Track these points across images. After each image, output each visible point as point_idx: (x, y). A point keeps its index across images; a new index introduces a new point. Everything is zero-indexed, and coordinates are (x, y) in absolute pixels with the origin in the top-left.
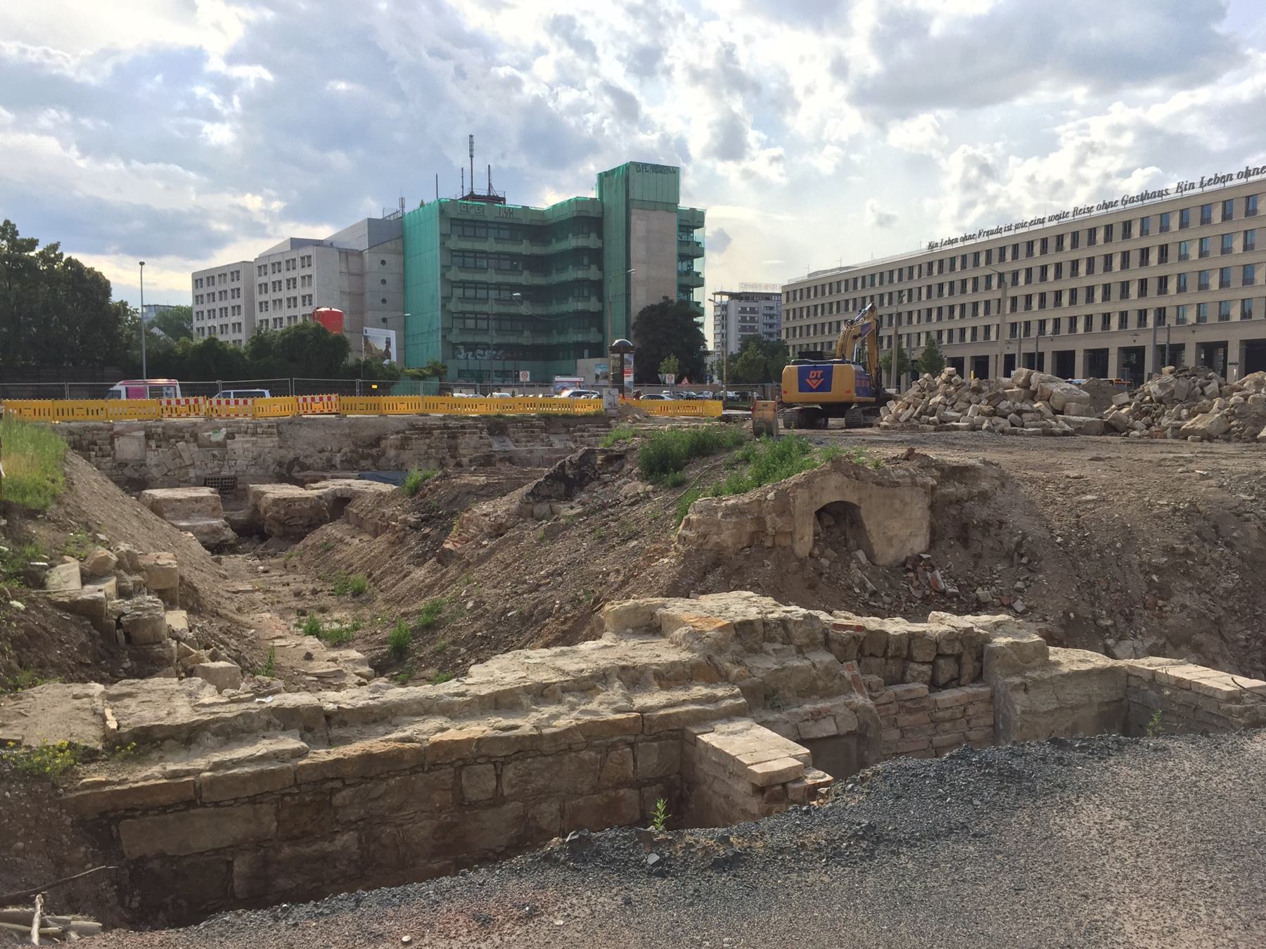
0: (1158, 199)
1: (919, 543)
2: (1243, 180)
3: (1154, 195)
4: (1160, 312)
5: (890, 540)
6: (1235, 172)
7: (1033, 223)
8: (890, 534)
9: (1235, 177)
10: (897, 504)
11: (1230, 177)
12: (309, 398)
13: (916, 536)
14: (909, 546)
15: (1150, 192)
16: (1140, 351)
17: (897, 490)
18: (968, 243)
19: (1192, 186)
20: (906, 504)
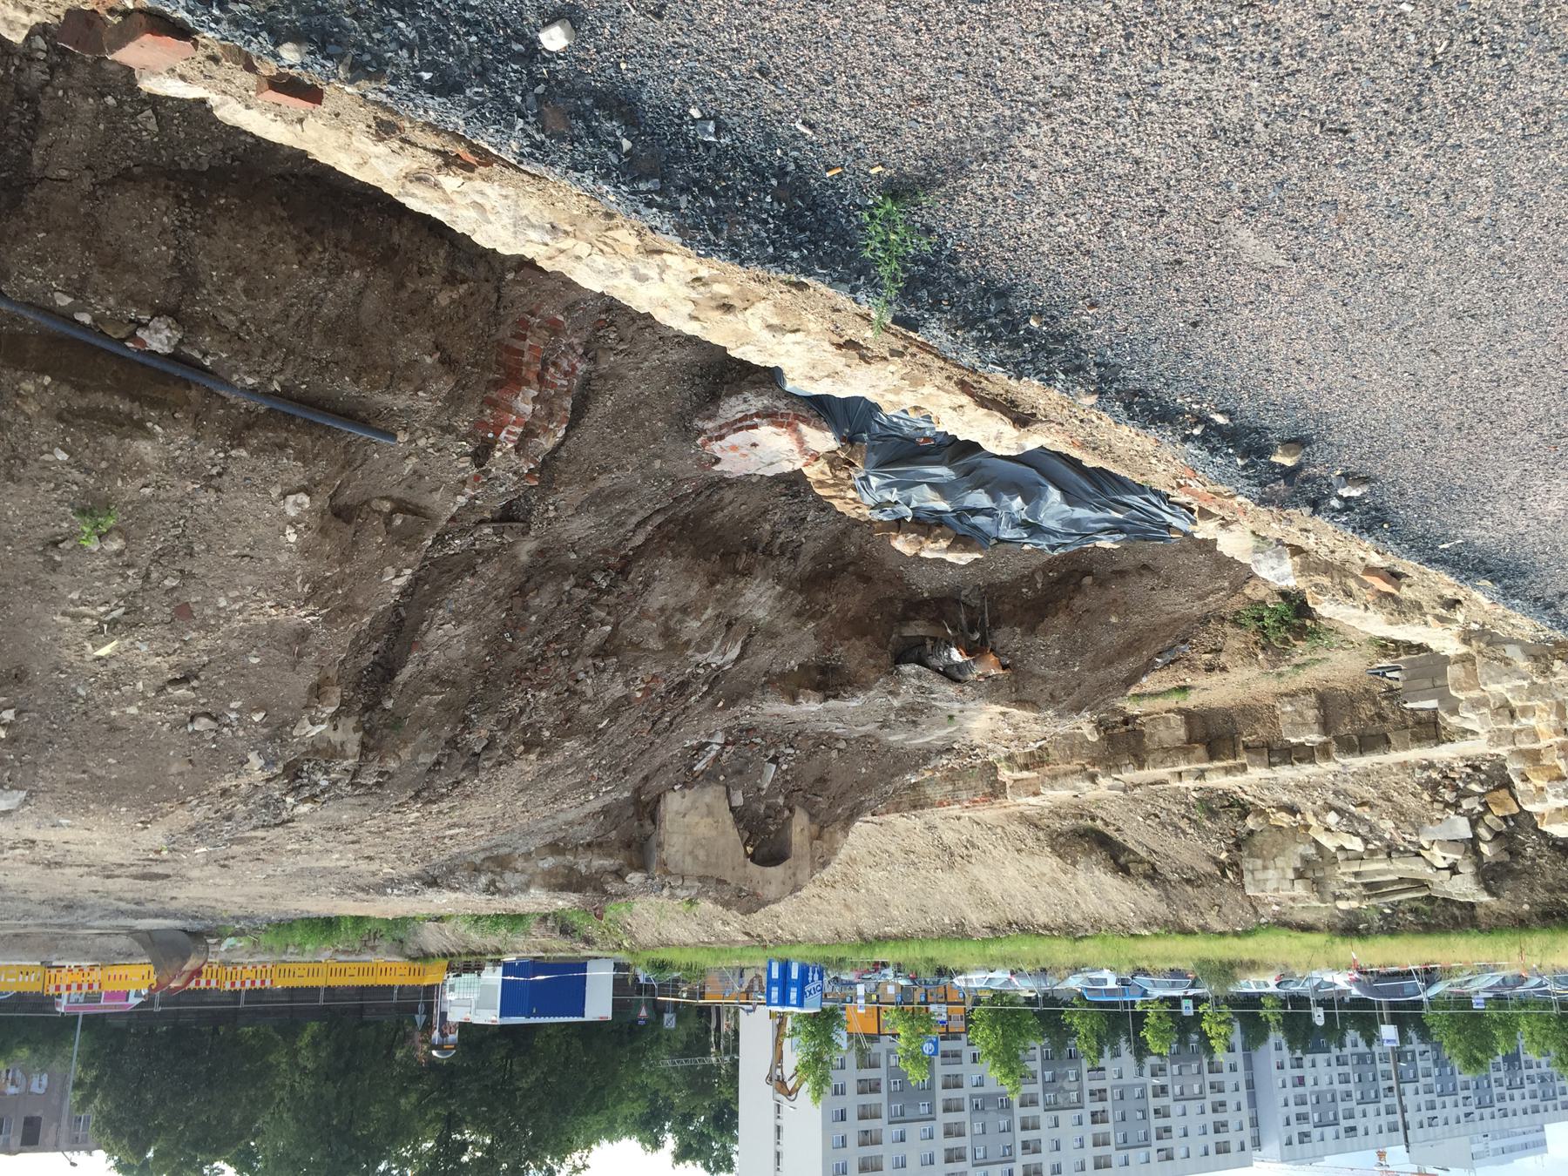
1: (674, 803)
5: (710, 812)
8: (710, 820)
10: (701, 854)
12: (258, 985)
13: (677, 813)
14: (687, 802)
17: (702, 872)
20: (691, 853)
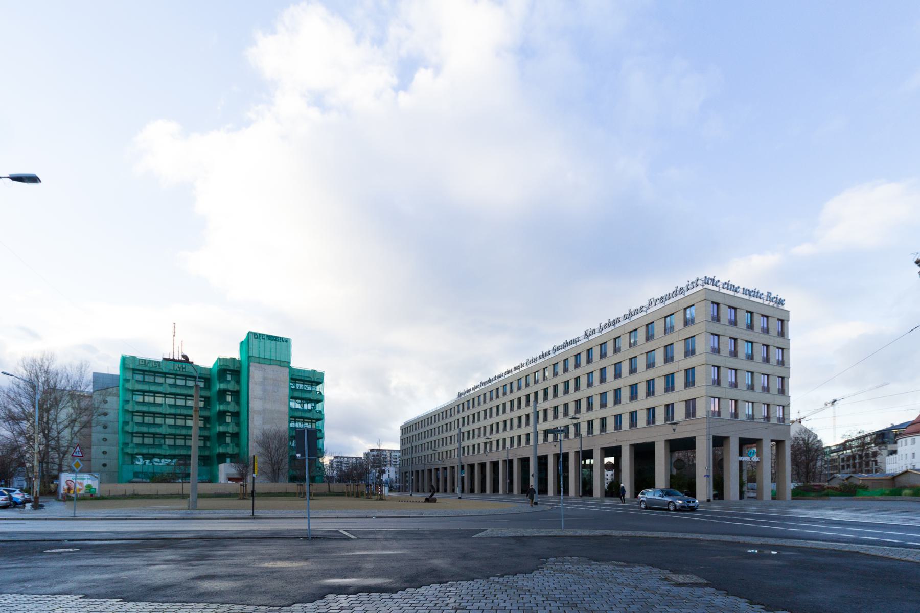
0: (574, 345)
2: (628, 321)
3: (571, 343)
4: (589, 424)
6: (621, 315)
7: (506, 373)
9: (621, 319)
11: (618, 320)
15: (568, 341)
16: (566, 456)
18: (476, 390)
19: (594, 332)
